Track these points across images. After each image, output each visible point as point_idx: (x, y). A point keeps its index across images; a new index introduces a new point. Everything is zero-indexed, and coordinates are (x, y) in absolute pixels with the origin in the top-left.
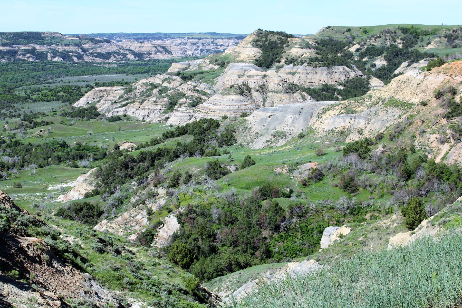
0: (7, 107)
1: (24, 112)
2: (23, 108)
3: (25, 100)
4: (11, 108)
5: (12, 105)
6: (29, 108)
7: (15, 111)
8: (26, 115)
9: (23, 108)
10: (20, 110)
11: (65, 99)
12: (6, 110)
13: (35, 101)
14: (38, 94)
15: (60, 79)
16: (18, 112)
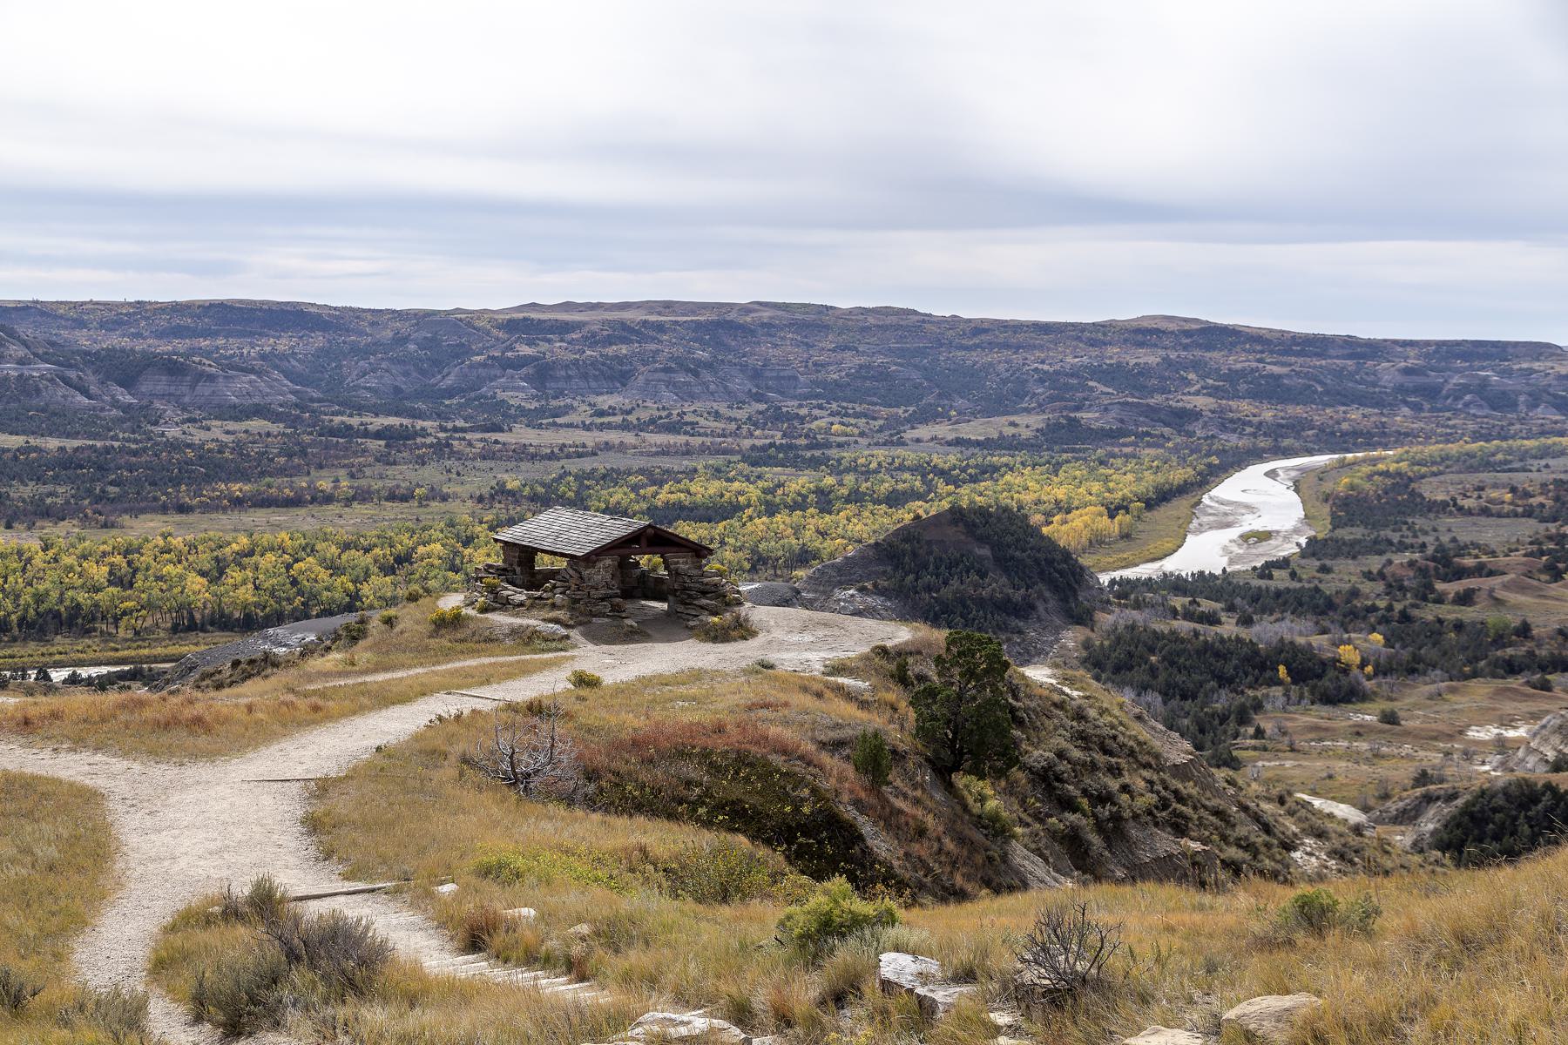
0: (1396, 523)
1: (1437, 539)
2: (1435, 530)
3: (1444, 509)
4: (1404, 528)
5: (1410, 520)
6: (1449, 530)
7: (1415, 536)
8: (1440, 548)
9: (1435, 530)
10: (1426, 533)
11: (1546, 513)
12: (1394, 531)
13: (1470, 512)
14: (1480, 497)
15: (1543, 462)
16: (1422, 539)
